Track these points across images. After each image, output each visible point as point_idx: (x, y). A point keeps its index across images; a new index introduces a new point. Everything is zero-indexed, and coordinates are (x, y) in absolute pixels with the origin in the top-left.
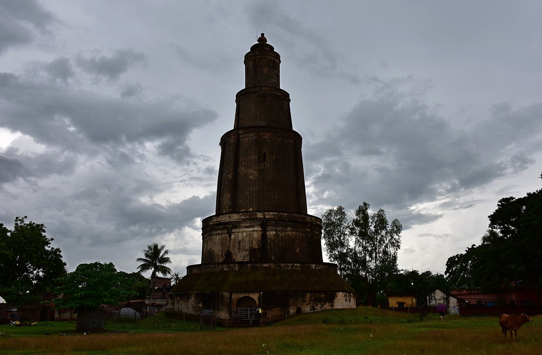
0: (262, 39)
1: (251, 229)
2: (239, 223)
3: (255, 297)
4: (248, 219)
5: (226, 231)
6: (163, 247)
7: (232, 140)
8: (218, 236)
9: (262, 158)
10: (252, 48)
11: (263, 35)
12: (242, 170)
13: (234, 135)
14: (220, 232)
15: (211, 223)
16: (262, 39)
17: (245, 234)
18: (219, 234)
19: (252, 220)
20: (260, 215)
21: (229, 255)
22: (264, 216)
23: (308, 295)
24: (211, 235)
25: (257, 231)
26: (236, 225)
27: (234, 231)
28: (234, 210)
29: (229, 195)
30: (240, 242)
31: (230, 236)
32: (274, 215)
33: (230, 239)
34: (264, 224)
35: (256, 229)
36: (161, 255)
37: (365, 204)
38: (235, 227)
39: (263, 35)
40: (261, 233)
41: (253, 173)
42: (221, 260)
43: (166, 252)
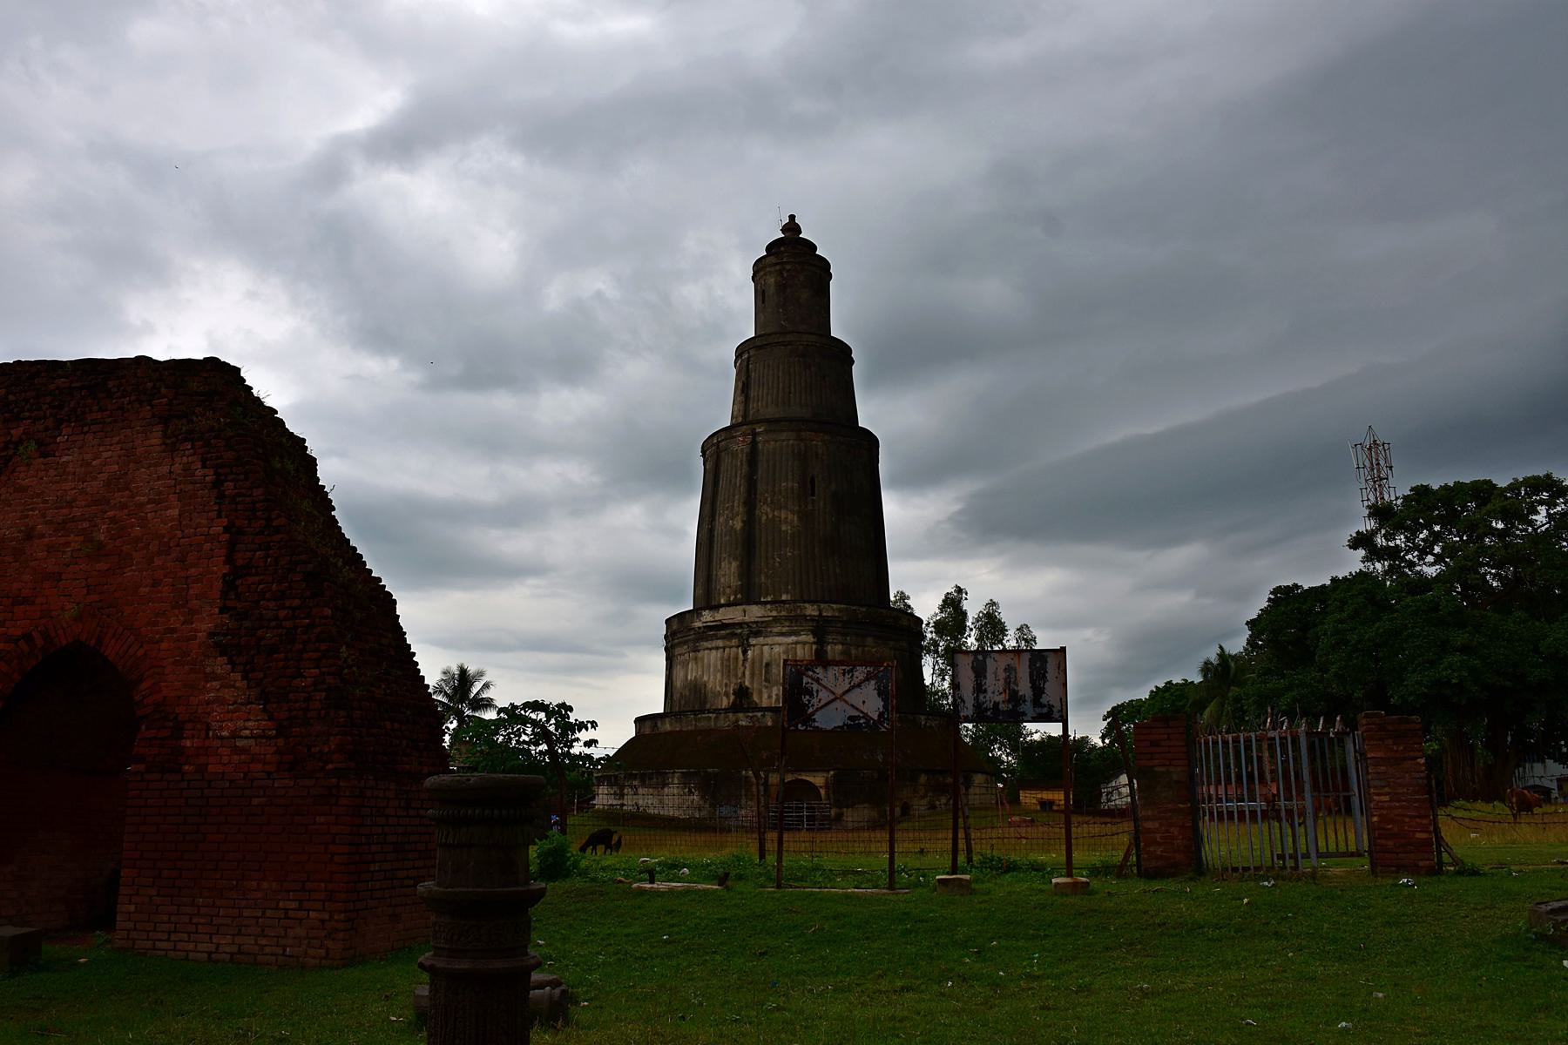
0: (792, 227)
1: (793, 639)
2: (768, 624)
3: (818, 780)
4: (787, 618)
5: (734, 642)
6: (481, 674)
7: (740, 445)
9: (808, 486)
10: (769, 248)
11: (792, 217)
12: (764, 512)
13: (744, 435)
14: (720, 643)
15: (698, 624)
16: (792, 227)
17: (777, 649)
19: (796, 621)
20: (811, 610)
21: (742, 693)
23: (923, 778)
24: (696, 650)
25: (804, 643)
26: (758, 629)
27: (753, 641)
28: (748, 595)
29: (734, 564)
30: (768, 665)
31: (745, 652)
32: (839, 610)
33: (745, 660)
34: (820, 629)
35: (803, 638)
36: (475, 690)
37: (959, 590)
38: (757, 634)
39: (792, 217)
41: (788, 520)
42: (725, 703)
43: (486, 686)
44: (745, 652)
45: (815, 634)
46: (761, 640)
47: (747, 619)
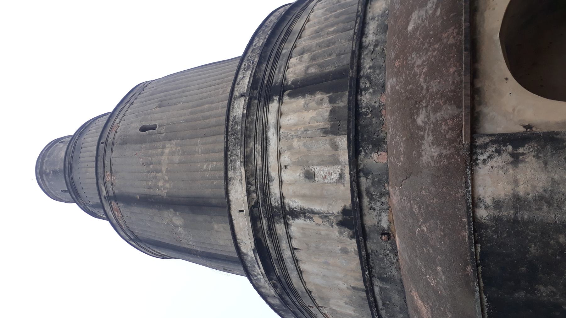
1: (272, 135)
5: (280, 228)
8: (302, 266)
18: (296, 261)
22: (242, 95)
25: (280, 114)
29: (216, 226)
31: (295, 214)
35: (272, 119)
40: (286, 99)
44: (295, 214)
45: (268, 100)
46: (275, 189)
47: (245, 208)
